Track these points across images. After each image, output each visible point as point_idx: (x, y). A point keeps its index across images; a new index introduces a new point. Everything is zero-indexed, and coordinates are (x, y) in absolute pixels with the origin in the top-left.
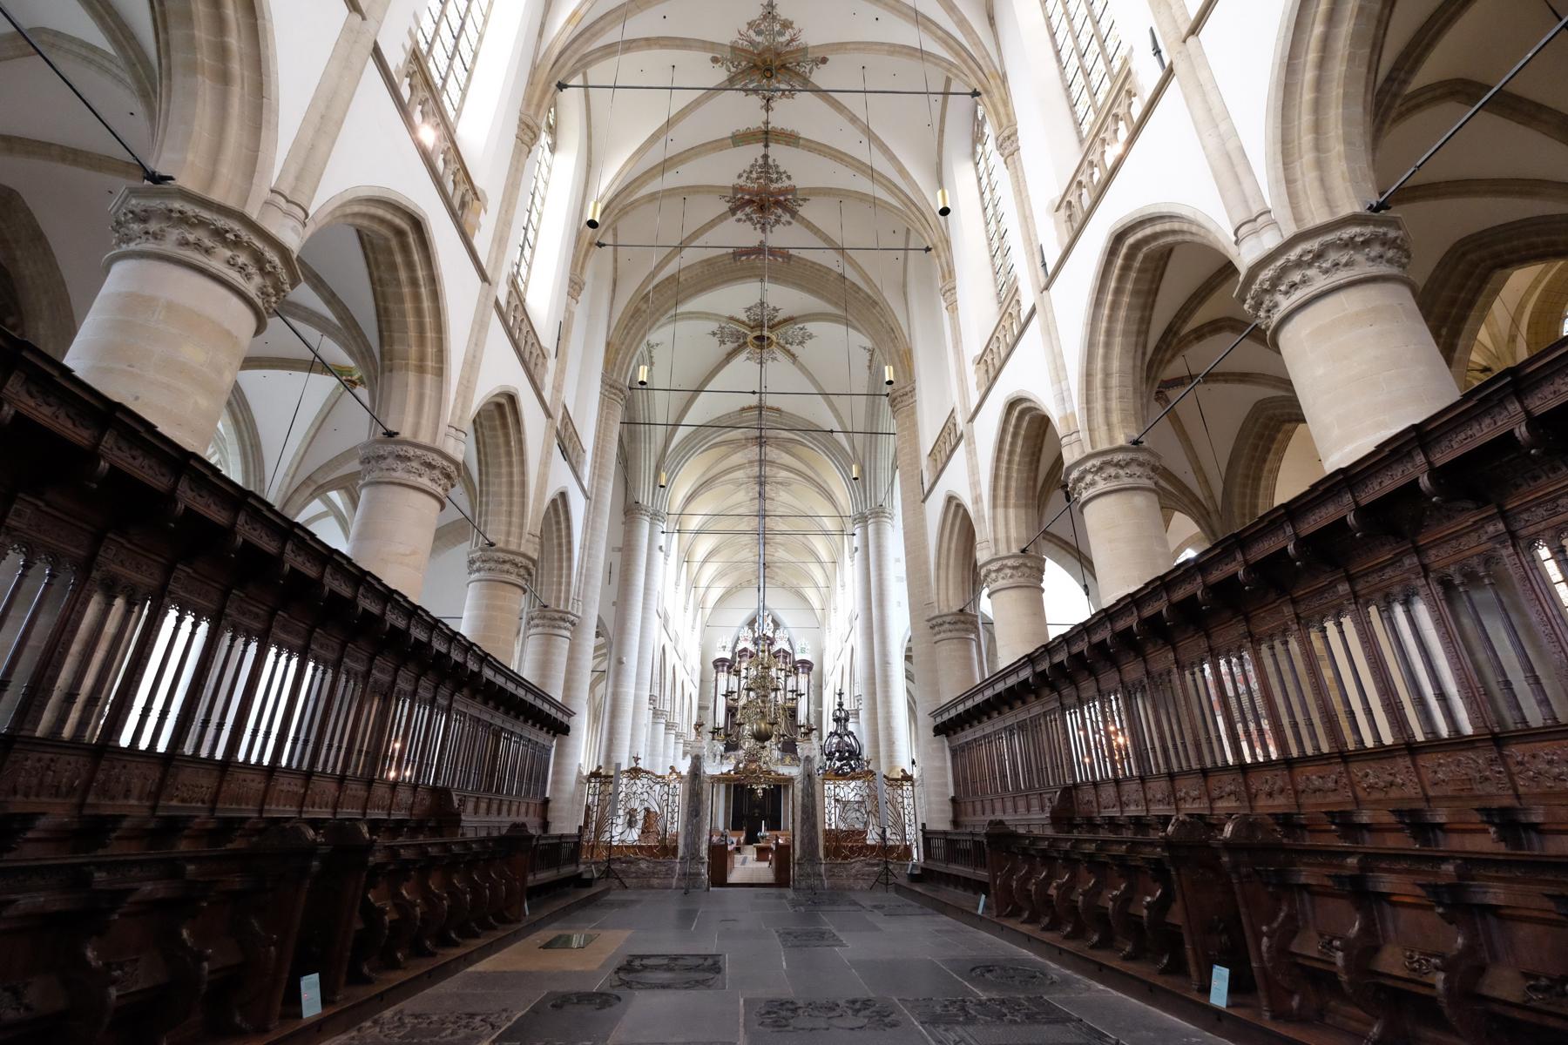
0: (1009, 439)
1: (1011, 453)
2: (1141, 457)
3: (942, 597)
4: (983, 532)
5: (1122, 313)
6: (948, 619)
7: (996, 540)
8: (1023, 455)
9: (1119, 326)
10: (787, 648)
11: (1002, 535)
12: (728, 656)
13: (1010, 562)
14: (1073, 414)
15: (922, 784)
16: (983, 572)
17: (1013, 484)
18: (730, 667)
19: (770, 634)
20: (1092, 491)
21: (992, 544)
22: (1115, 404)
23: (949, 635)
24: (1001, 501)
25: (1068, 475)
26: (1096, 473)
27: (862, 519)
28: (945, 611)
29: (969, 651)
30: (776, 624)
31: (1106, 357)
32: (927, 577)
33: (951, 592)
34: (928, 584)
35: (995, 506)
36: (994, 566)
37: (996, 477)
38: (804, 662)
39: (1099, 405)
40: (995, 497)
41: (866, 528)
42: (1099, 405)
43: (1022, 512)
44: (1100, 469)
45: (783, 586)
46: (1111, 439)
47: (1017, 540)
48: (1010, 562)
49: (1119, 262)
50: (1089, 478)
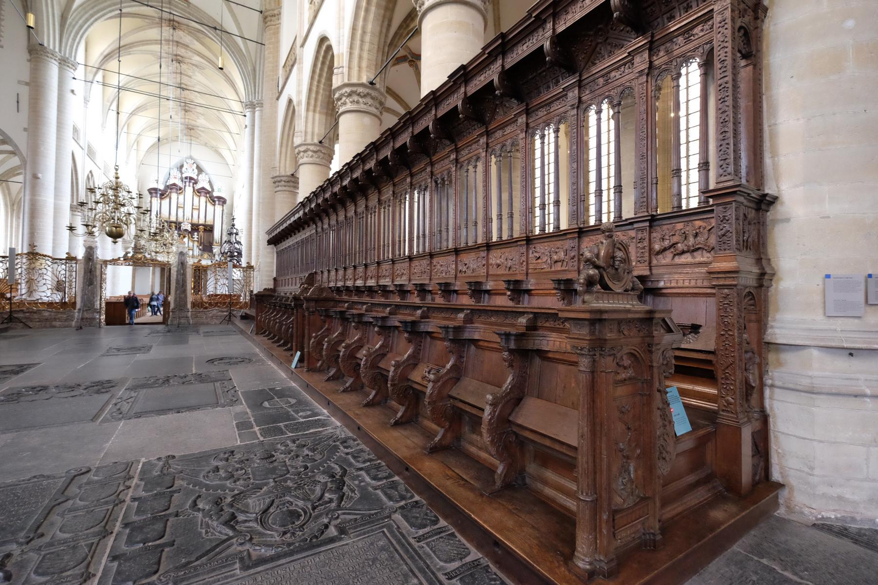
0: (319, 65)
1: (320, 75)
2: (373, 93)
3: (282, 165)
4: (300, 124)
6: (284, 179)
7: (306, 132)
10: (208, 188)
11: (310, 130)
12: (162, 187)
13: (312, 148)
14: (343, 54)
15: (259, 271)
16: (297, 151)
17: (320, 97)
18: (162, 195)
19: (196, 178)
21: (303, 134)
22: (365, 55)
23: (284, 188)
24: (311, 108)
26: (348, 96)
27: (252, 106)
28: (283, 174)
30: (200, 170)
31: (365, 19)
32: (274, 151)
33: (288, 162)
34: (275, 155)
35: (308, 110)
36: (302, 149)
37: (310, 90)
38: (219, 198)
39: (356, 52)
40: (308, 104)
41: (254, 113)
42: (356, 52)
43: (324, 117)
44: (350, 95)
45: (206, 145)
46: (359, 77)
47: (318, 135)
48: (312, 148)
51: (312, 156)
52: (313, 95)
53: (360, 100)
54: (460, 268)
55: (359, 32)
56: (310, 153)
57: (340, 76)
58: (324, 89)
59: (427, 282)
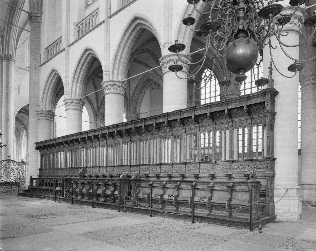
0: (83, 60)
5: (130, 41)
7: (72, 93)
8: (86, 67)
9: (128, 45)
11: (74, 92)
20: (109, 91)
21: (70, 94)
22: (121, 68)
24: (75, 80)
25: (103, 84)
28: (44, 109)
29: (51, 124)
31: (122, 52)
35: (73, 81)
43: (82, 86)
46: (118, 78)
49: (134, 26)
50: (109, 87)
52: (77, 74)
55: (119, 57)
57: (108, 76)
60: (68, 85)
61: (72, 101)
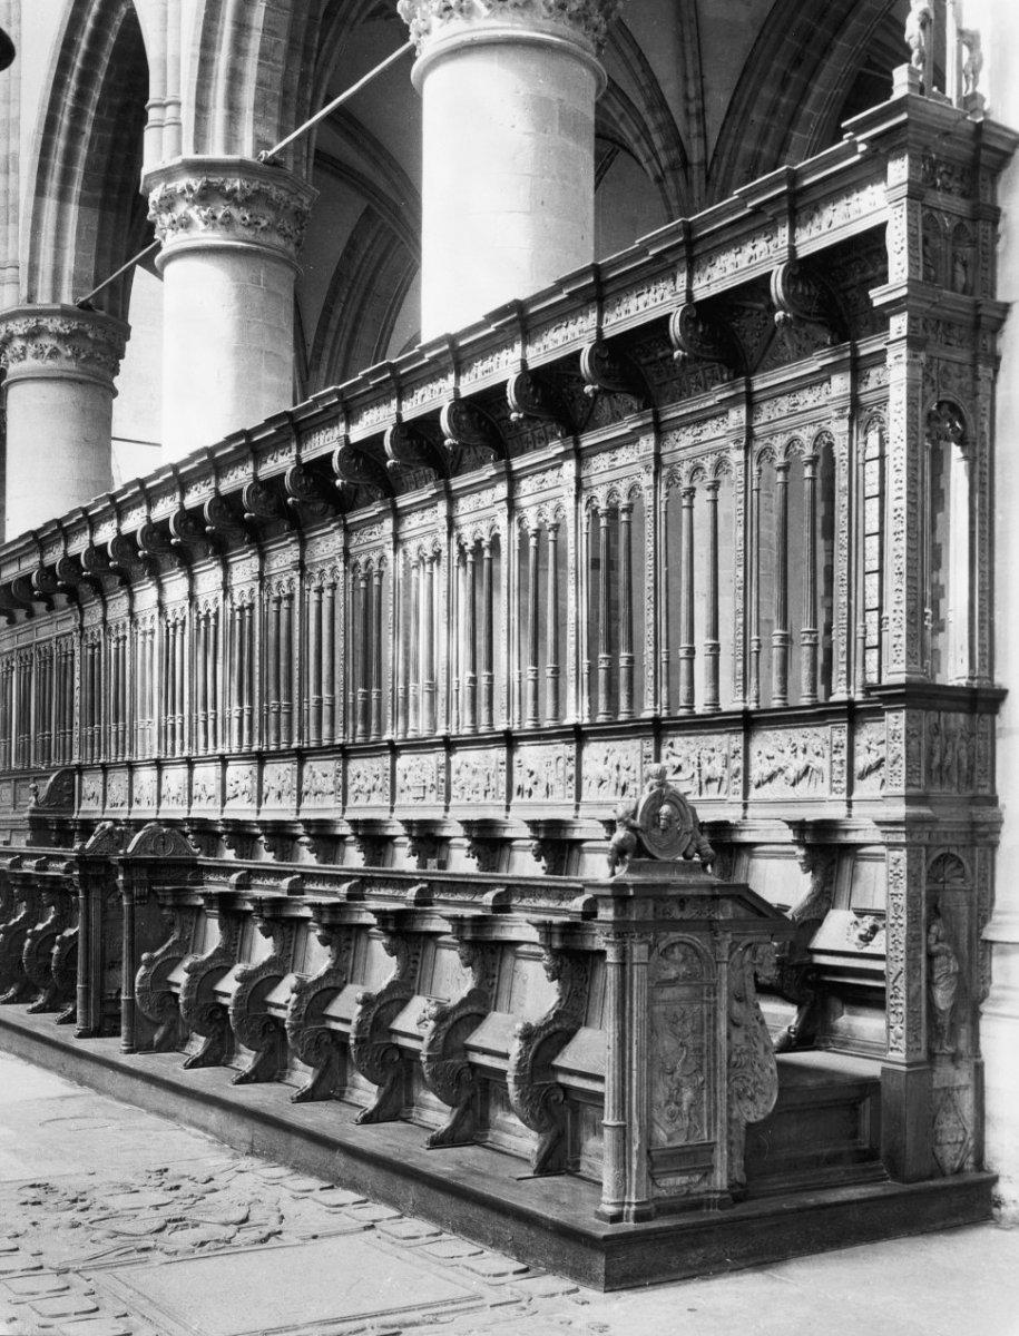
7: (33, 269)
22: (251, 69)
24: (53, 184)
25: (148, 190)
35: (40, 191)
39: (222, 58)
40: (43, 170)
42: (222, 58)
47: (78, 280)
48: (54, 324)
51: (54, 354)
53: (237, 214)
54: (517, 782)
56: (49, 343)
57: (168, 132)
58: (97, 124)
59: (437, 815)
60: (16, 221)
61: (32, 322)
